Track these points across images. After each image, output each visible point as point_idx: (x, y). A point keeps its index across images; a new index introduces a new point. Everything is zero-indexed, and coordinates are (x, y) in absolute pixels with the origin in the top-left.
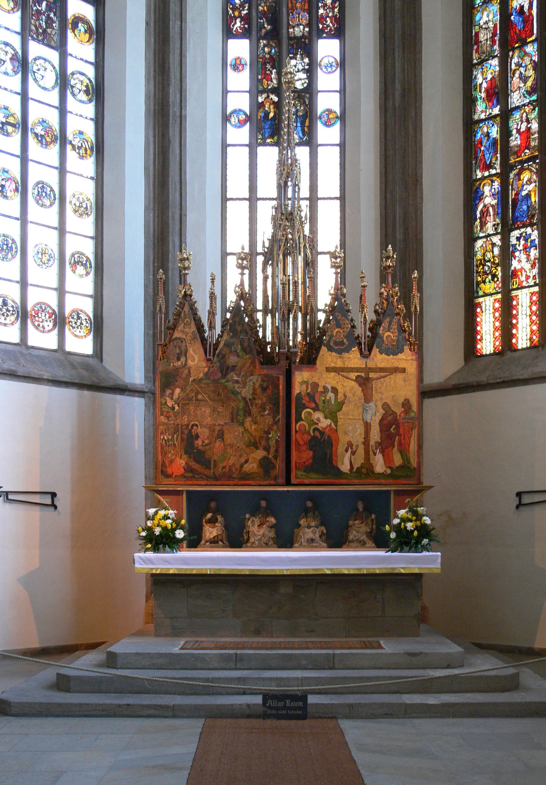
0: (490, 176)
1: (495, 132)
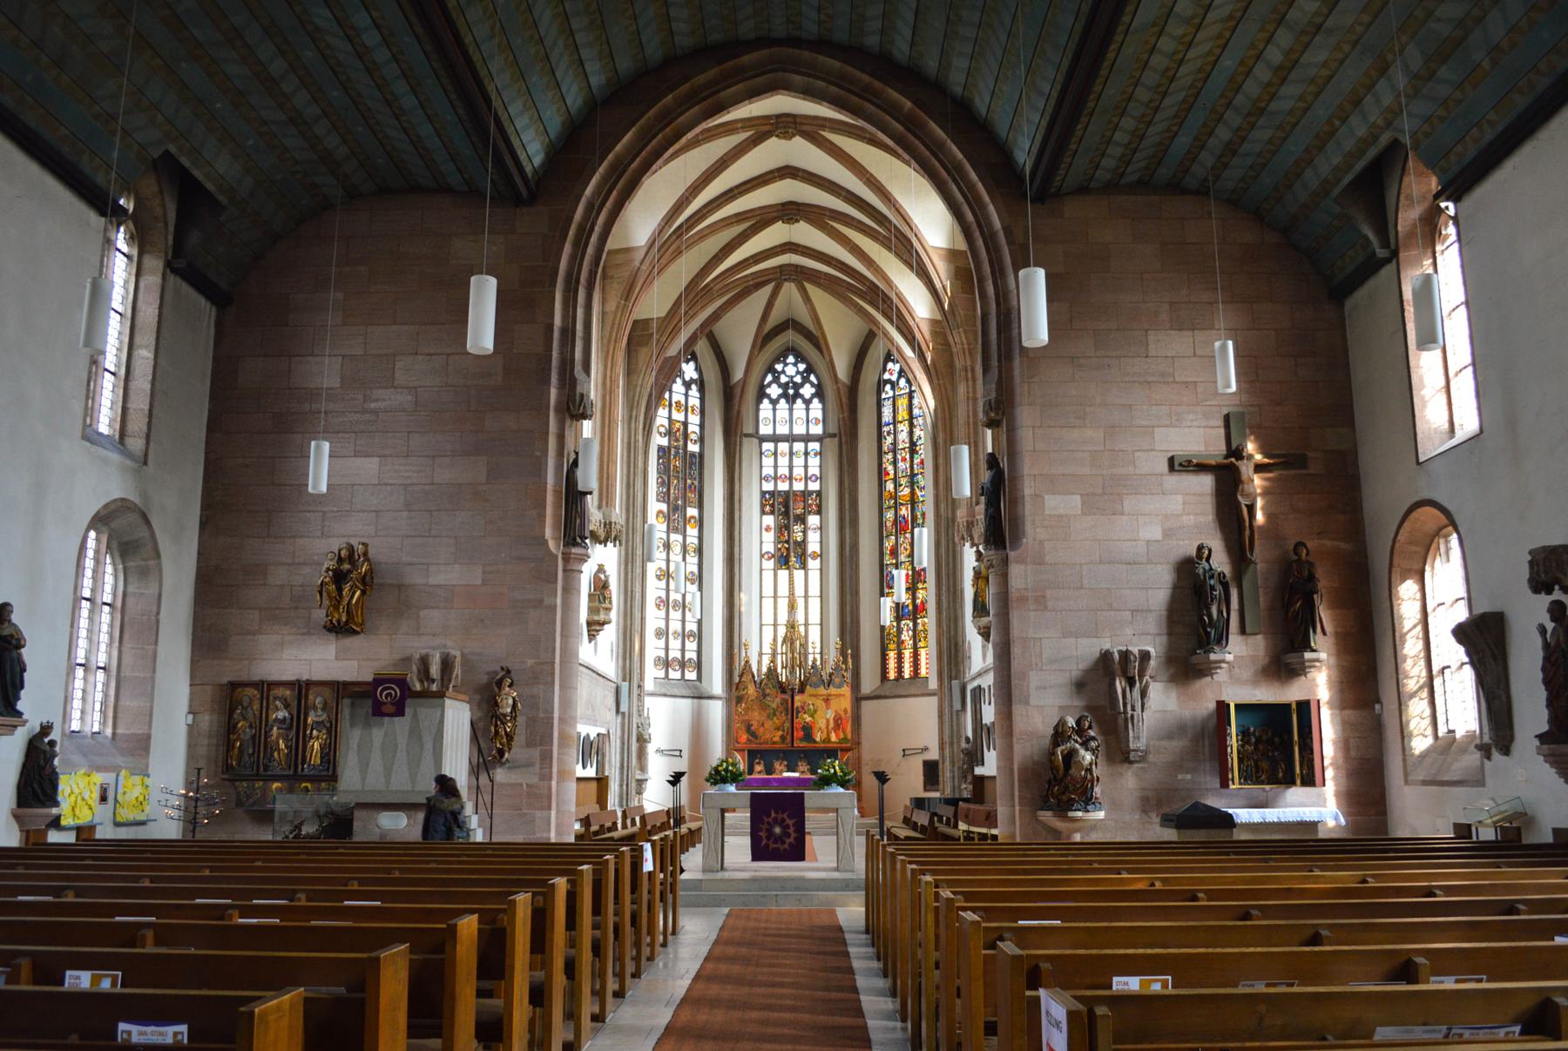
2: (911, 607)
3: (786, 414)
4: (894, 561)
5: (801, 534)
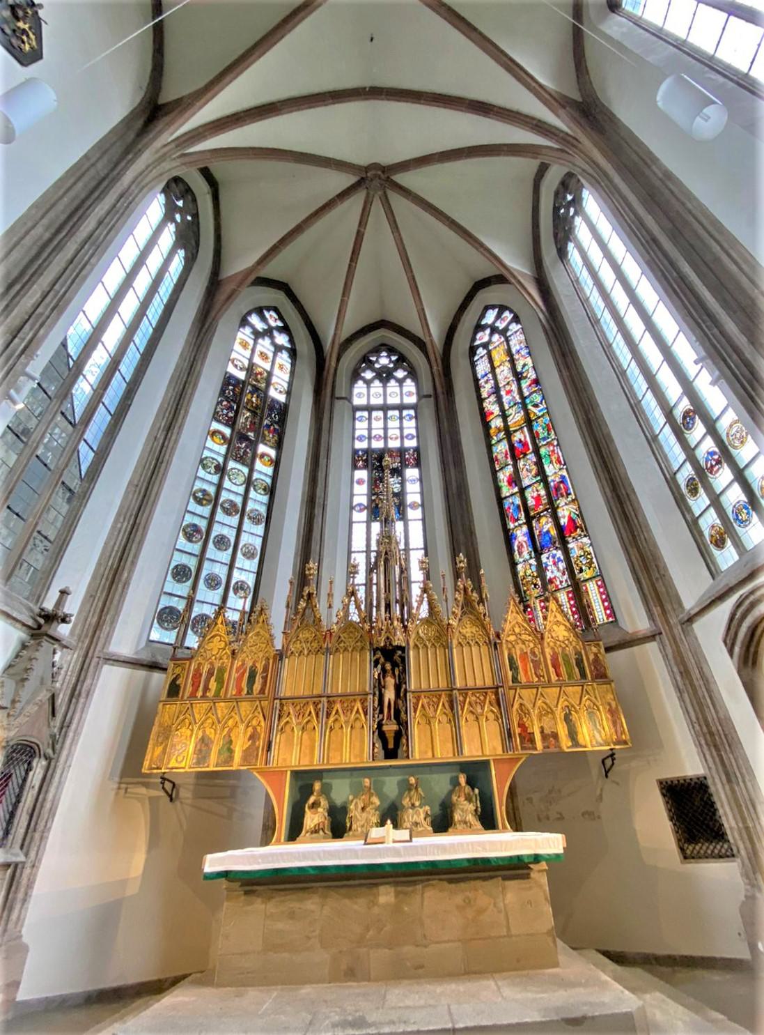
0: (520, 525)
1: (518, 501)
2: (554, 532)
3: (381, 390)
4: (516, 489)
5: (398, 486)
